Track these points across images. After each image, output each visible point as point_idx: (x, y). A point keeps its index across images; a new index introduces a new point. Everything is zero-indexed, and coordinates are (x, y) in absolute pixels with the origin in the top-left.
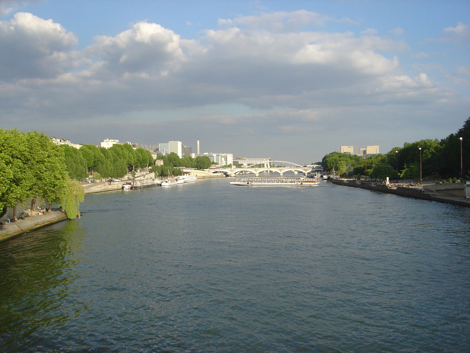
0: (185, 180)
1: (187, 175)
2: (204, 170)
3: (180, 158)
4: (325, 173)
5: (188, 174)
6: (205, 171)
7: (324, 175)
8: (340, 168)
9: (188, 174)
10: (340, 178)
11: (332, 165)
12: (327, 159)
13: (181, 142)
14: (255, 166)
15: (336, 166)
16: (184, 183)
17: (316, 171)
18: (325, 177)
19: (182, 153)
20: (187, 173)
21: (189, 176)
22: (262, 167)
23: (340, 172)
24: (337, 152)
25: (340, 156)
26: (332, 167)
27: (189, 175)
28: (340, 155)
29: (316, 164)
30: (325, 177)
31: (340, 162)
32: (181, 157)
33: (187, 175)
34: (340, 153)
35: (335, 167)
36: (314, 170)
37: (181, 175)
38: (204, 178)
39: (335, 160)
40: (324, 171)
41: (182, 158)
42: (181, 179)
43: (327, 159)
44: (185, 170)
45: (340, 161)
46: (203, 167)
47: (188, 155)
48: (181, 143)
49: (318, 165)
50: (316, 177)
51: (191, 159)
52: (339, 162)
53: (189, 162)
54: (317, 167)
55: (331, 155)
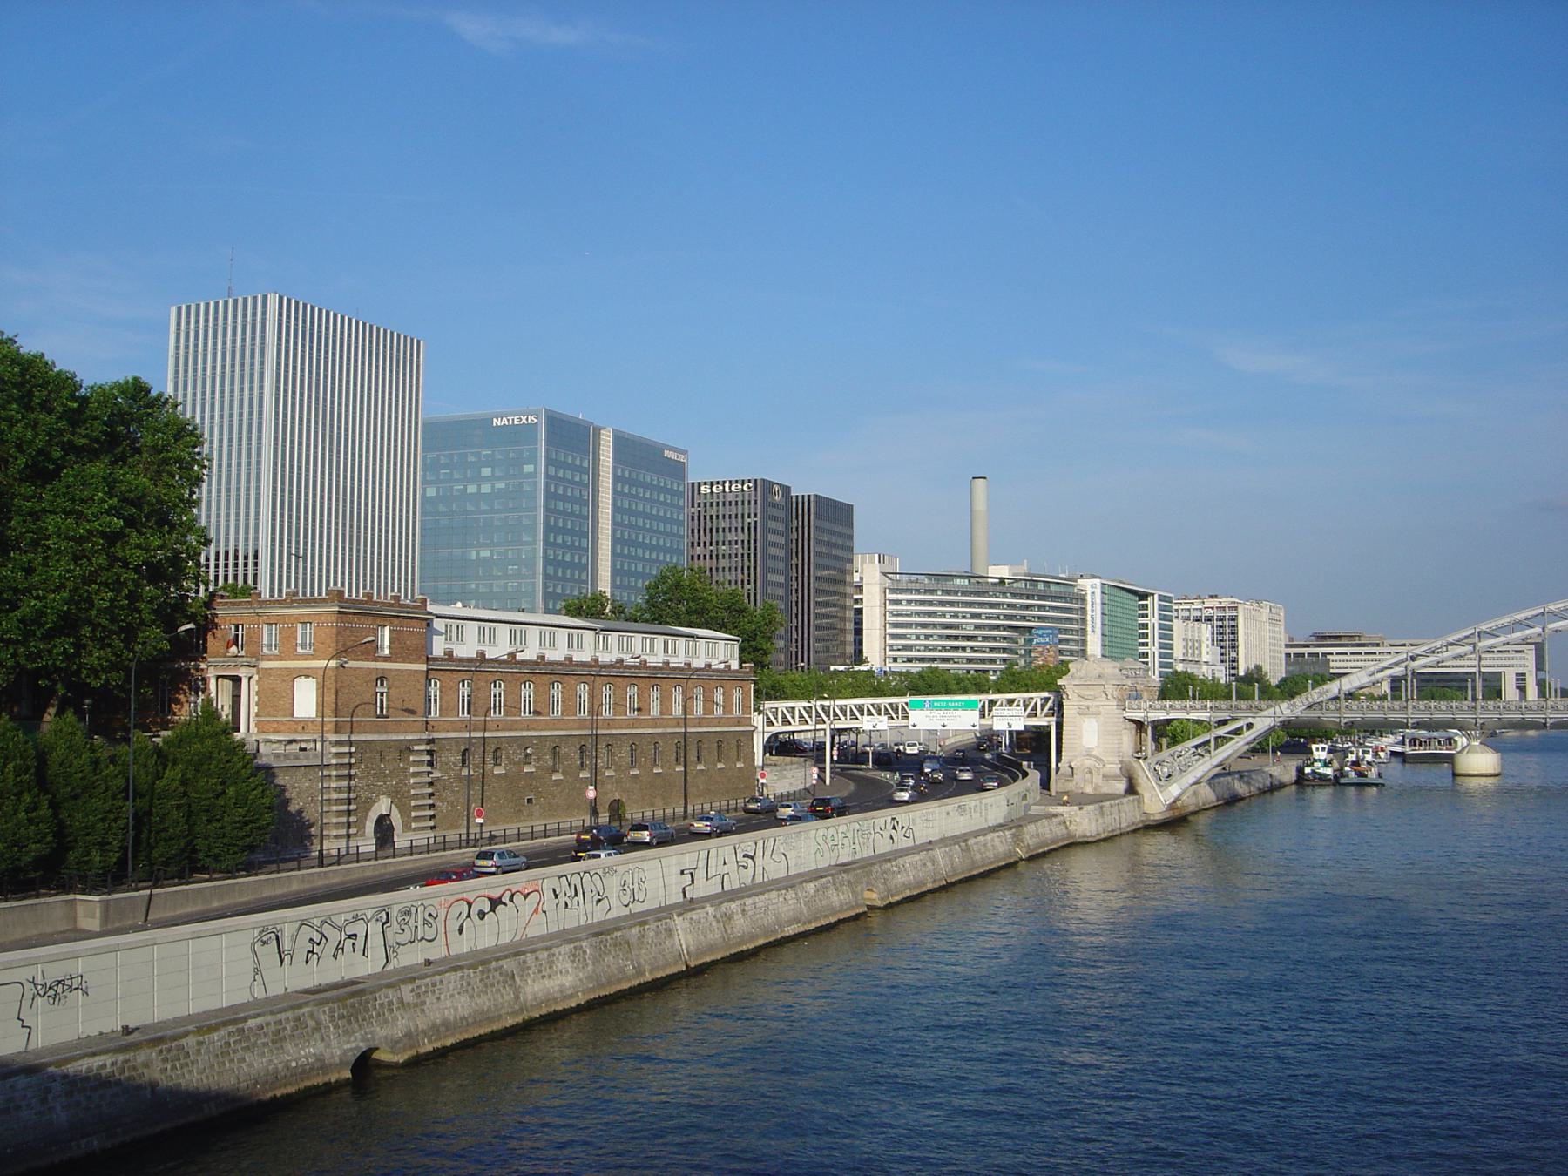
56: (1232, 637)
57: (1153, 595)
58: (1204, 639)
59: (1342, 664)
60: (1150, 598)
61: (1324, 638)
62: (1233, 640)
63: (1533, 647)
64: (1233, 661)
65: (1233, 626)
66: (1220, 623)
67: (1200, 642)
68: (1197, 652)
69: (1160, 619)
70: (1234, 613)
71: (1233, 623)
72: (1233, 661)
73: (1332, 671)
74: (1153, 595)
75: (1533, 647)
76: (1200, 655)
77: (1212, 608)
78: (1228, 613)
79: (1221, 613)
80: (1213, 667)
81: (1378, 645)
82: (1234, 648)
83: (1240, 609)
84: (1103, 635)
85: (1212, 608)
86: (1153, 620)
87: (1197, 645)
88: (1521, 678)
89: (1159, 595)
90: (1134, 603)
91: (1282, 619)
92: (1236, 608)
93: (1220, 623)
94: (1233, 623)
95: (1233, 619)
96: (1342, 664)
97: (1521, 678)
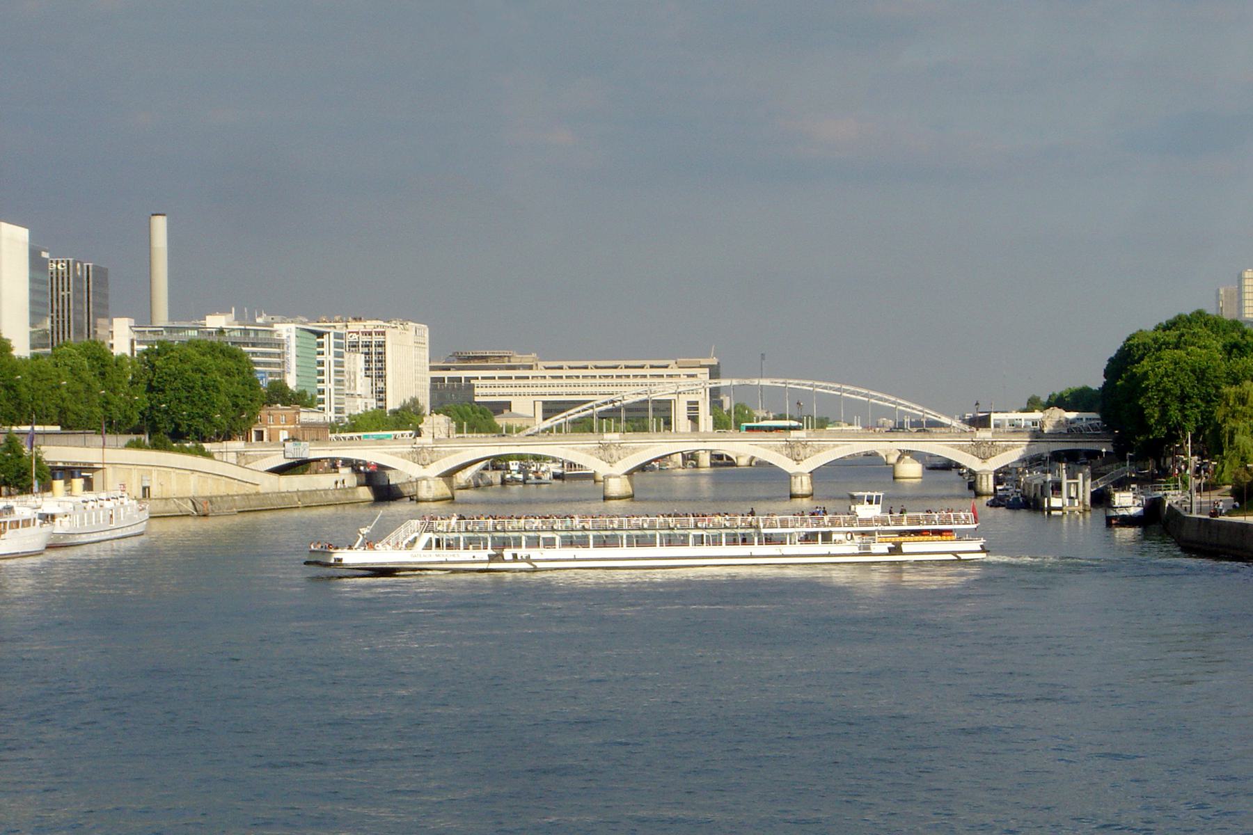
0: (61, 526)
1: (69, 492)
2: (207, 446)
3: (15, 353)
4: (1128, 470)
5: (78, 483)
6: (209, 455)
7: (1122, 485)
8: (1237, 438)
9: (78, 483)
10: (1229, 513)
11: (1174, 413)
12: (1138, 369)
13: (27, 231)
14: (602, 416)
15: (1208, 417)
16: (54, 554)
17: (1057, 457)
18: (1127, 502)
19: (35, 317)
20: (69, 472)
21: (90, 496)
22: (652, 422)
23: (1236, 462)
24: (1211, 311)
25: (1235, 346)
26: (1179, 426)
27: (89, 485)
28: (1236, 336)
29: (1059, 402)
30: (1127, 502)
31: (1233, 389)
32: (21, 349)
33: (69, 492)
34: (1236, 325)
35: (1199, 430)
36: (1045, 449)
37: (26, 490)
38: (201, 509)
39: (1201, 375)
40: (1118, 455)
41: (36, 357)
42: (27, 523)
43: (1138, 369)
44: (58, 452)
45: (1236, 381)
46: (199, 423)
47: (79, 331)
48: (22, 234)
49: (1072, 415)
50: (1056, 502)
51: (100, 359)
52: (1225, 389)
53: (89, 388)
54: (1070, 430)
55: (1172, 336)
56: (379, 365)
57: (329, 333)
58: (358, 370)
59: (488, 391)
60: (326, 337)
61: (470, 359)
62: (380, 369)
63: (707, 370)
64: (381, 392)
65: (380, 353)
66: (366, 350)
67: (355, 373)
68: (353, 384)
69: (335, 357)
70: (381, 338)
71: (380, 350)
72: (381, 392)
73: (477, 399)
74: (329, 333)
75: (707, 370)
76: (355, 388)
77: (358, 333)
78: (375, 339)
79: (366, 339)
80: (366, 400)
81: (530, 368)
82: (382, 377)
83: (388, 332)
84: (297, 376)
85: (358, 333)
86: (329, 358)
87: (352, 377)
88: (693, 407)
89: (335, 333)
90: (313, 342)
91: (427, 342)
92: (383, 333)
93: (366, 350)
94: (380, 350)
95: (381, 345)
96: (488, 391)
97: (693, 407)
